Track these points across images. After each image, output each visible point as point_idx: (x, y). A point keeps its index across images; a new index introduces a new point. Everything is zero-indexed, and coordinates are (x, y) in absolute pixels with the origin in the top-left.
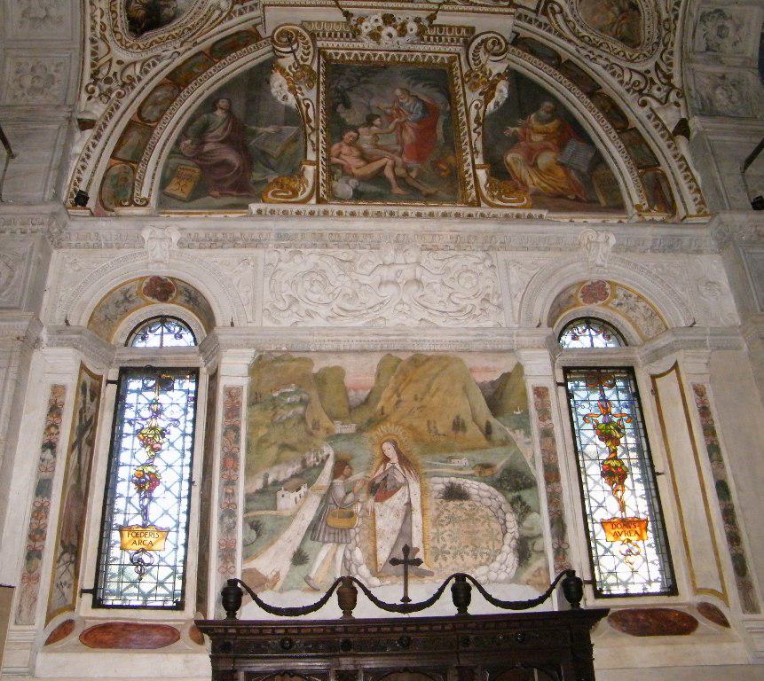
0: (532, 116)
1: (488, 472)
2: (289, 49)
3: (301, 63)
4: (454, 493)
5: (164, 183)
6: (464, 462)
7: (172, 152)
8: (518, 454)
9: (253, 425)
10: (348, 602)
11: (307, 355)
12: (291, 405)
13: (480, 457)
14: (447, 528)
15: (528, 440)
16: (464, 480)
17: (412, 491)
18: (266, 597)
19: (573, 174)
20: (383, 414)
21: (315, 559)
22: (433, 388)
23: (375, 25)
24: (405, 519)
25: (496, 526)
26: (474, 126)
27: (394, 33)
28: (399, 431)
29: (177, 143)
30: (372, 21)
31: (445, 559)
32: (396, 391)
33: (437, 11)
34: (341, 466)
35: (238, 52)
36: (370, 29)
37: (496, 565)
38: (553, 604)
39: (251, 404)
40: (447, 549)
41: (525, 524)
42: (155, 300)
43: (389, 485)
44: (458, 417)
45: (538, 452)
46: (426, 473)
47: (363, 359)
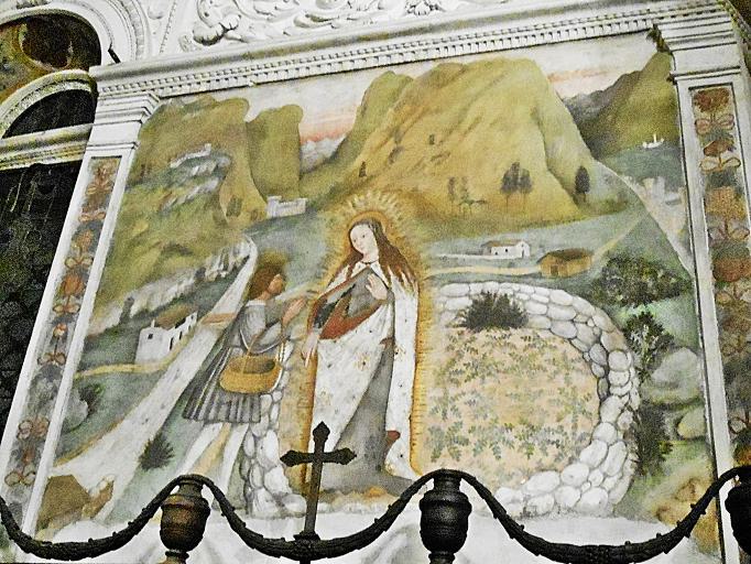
1: (573, 268)
4: (491, 314)
6: (520, 250)
8: (649, 228)
9: (126, 219)
13: (557, 239)
14: (465, 387)
15: (672, 196)
16: (516, 287)
20: (362, 174)
22: (469, 119)
24: (375, 377)
25: (585, 383)
28: (388, 206)
32: (395, 133)
37: (577, 471)
40: (463, 433)
41: (658, 375)
42: (48, 67)
43: (354, 305)
44: (515, 167)
46: (432, 278)
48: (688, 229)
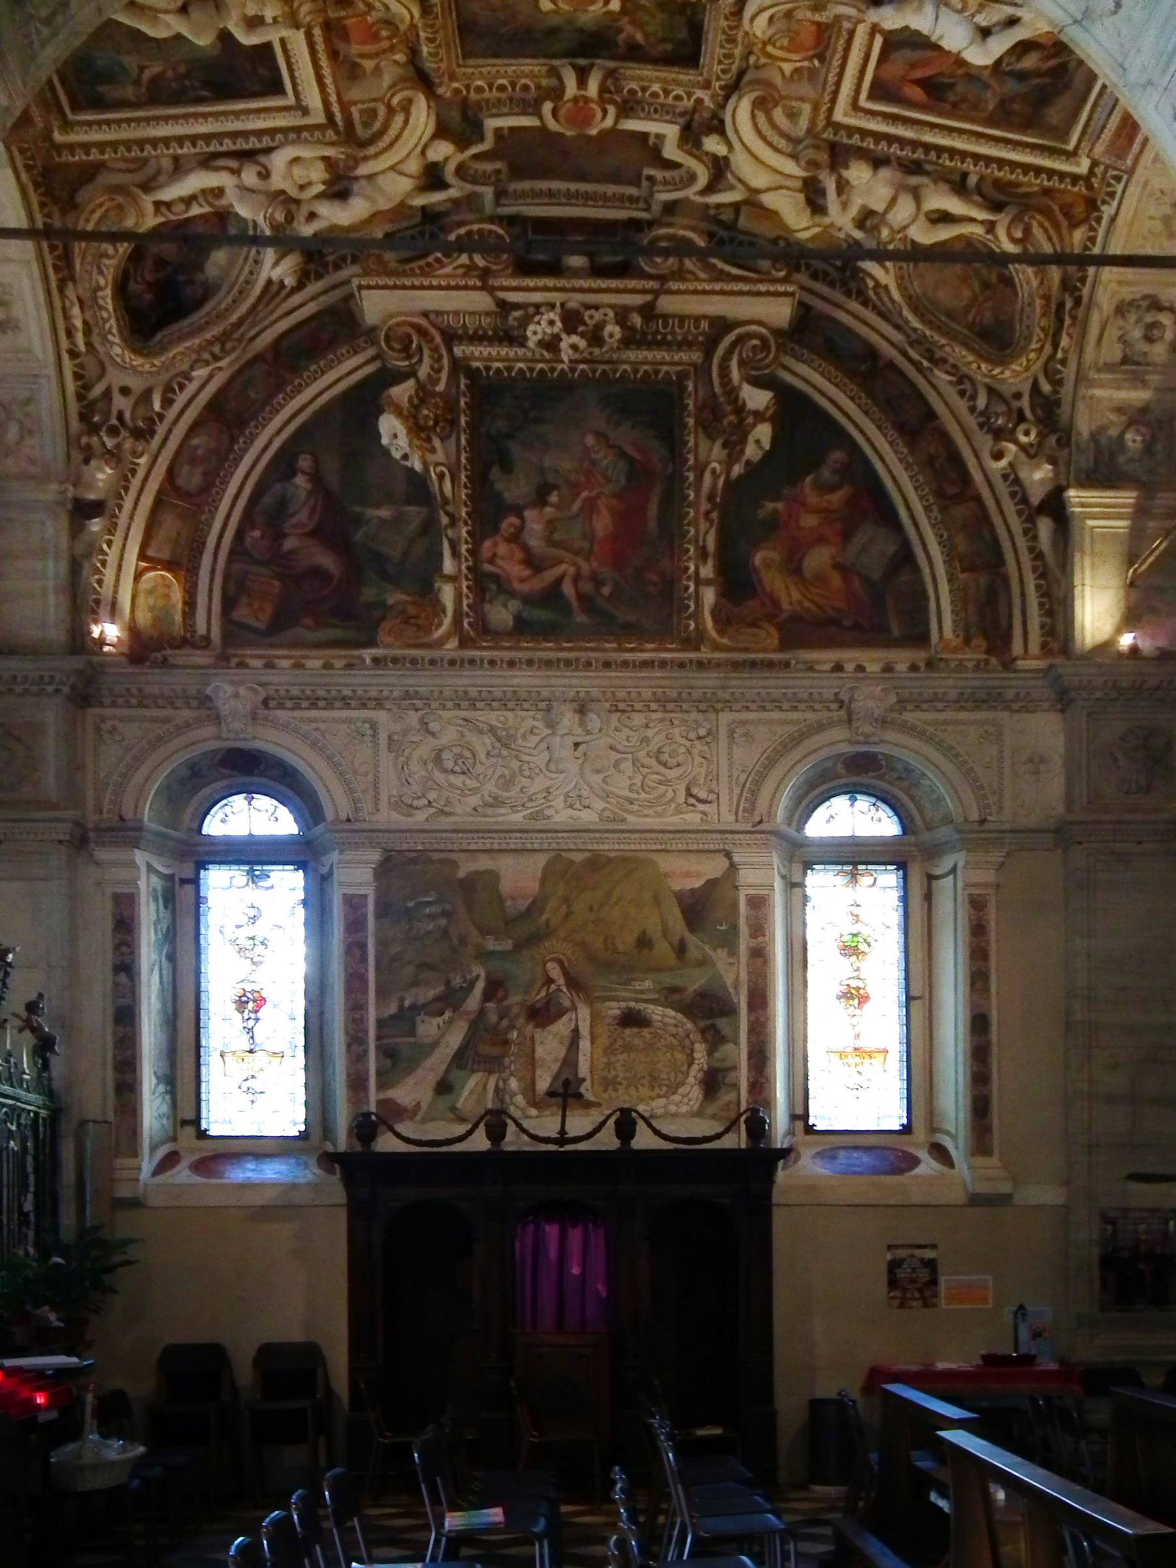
0: (809, 479)
1: (677, 997)
2: (406, 363)
3: (429, 387)
4: (632, 1019)
5: (228, 604)
6: (648, 984)
7: (232, 552)
9: (382, 943)
10: (496, 1133)
11: (453, 856)
12: (432, 917)
13: (668, 980)
14: (620, 1057)
15: (731, 960)
17: (580, 1016)
18: (404, 1128)
19: (857, 583)
20: (548, 927)
21: (463, 1087)
23: (549, 330)
25: (680, 1056)
26: (705, 506)
27: (582, 344)
28: (565, 949)
29: (239, 535)
30: (544, 323)
31: (616, 1090)
32: (566, 900)
33: (657, 293)
34: (495, 989)
35: (322, 363)
36: (540, 336)
37: (676, 1098)
38: (737, 1140)
39: (379, 916)
41: (717, 1055)
43: (553, 1009)
44: (644, 932)
45: (743, 976)
46: (597, 997)
47: (524, 860)
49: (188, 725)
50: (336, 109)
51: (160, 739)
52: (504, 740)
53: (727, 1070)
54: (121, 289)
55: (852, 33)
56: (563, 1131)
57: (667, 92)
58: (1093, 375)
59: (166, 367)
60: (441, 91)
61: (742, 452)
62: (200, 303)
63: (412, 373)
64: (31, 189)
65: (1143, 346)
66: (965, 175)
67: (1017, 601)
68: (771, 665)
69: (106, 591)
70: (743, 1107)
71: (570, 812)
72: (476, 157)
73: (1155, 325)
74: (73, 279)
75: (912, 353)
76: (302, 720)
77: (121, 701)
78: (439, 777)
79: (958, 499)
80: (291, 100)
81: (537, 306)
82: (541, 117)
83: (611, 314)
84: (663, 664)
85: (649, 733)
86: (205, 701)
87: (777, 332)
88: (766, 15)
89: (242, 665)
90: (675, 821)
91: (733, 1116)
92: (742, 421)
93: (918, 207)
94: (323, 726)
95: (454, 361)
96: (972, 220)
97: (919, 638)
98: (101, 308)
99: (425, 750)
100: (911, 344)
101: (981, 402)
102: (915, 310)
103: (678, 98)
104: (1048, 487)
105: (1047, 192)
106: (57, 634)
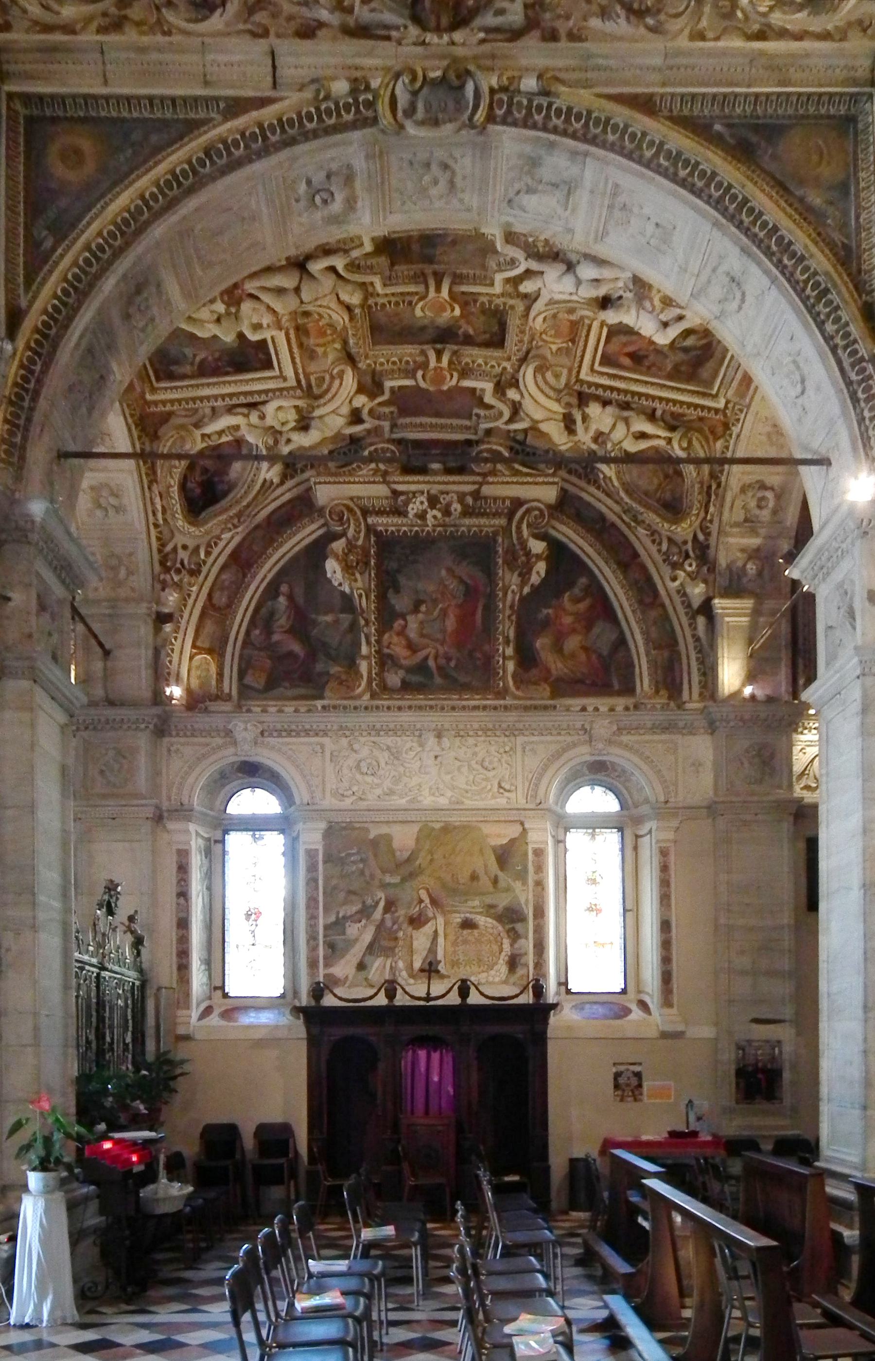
1: (493, 911)
4: (468, 924)
5: (242, 674)
6: (476, 903)
9: (327, 879)
10: (391, 994)
11: (366, 825)
13: (488, 900)
19: (594, 657)
25: (495, 948)
26: (508, 612)
28: (431, 883)
29: (248, 633)
32: (431, 852)
34: (390, 906)
37: (492, 972)
38: (527, 998)
41: (516, 946)
43: (422, 919)
44: (474, 872)
45: (531, 897)
48: (527, 900)
49: (219, 747)
50: (302, 376)
51: (203, 755)
52: (395, 755)
53: (520, 955)
54: (183, 487)
55: (590, 327)
56: (428, 993)
57: (486, 364)
58: (728, 529)
59: (207, 533)
60: (360, 365)
61: (529, 579)
62: (225, 494)
63: (344, 534)
64: (133, 427)
65: (757, 512)
66: (654, 410)
67: (685, 667)
68: (545, 708)
69: (174, 667)
70: (531, 978)
71: (433, 798)
72: (380, 404)
73: (763, 498)
74: (156, 482)
75: (625, 518)
76: (283, 744)
77: (181, 733)
78: (359, 777)
79: (652, 605)
80: (277, 373)
81: (414, 493)
82: (416, 380)
83: (455, 498)
84: (485, 708)
85: (477, 749)
86: (229, 733)
87: (549, 507)
88: (543, 316)
89: (249, 711)
90: (492, 803)
91: (525, 983)
92: (528, 560)
93: (628, 430)
94: (294, 747)
95: (368, 527)
96: (659, 437)
97: (628, 690)
98: (172, 498)
99: (351, 762)
100: (625, 512)
101: (664, 547)
102: (627, 492)
103: (493, 367)
104: (703, 598)
105: (701, 419)
106: (146, 694)
